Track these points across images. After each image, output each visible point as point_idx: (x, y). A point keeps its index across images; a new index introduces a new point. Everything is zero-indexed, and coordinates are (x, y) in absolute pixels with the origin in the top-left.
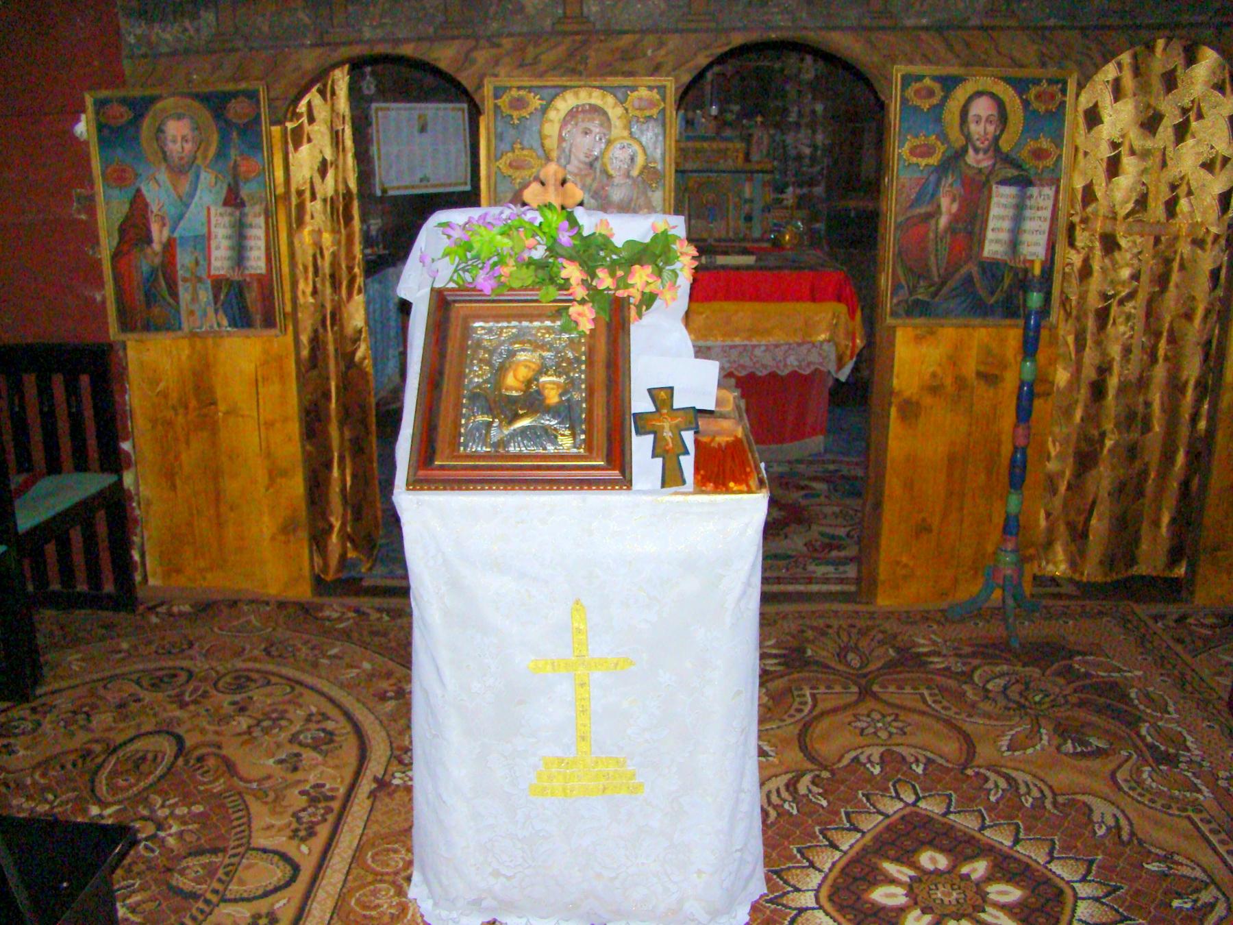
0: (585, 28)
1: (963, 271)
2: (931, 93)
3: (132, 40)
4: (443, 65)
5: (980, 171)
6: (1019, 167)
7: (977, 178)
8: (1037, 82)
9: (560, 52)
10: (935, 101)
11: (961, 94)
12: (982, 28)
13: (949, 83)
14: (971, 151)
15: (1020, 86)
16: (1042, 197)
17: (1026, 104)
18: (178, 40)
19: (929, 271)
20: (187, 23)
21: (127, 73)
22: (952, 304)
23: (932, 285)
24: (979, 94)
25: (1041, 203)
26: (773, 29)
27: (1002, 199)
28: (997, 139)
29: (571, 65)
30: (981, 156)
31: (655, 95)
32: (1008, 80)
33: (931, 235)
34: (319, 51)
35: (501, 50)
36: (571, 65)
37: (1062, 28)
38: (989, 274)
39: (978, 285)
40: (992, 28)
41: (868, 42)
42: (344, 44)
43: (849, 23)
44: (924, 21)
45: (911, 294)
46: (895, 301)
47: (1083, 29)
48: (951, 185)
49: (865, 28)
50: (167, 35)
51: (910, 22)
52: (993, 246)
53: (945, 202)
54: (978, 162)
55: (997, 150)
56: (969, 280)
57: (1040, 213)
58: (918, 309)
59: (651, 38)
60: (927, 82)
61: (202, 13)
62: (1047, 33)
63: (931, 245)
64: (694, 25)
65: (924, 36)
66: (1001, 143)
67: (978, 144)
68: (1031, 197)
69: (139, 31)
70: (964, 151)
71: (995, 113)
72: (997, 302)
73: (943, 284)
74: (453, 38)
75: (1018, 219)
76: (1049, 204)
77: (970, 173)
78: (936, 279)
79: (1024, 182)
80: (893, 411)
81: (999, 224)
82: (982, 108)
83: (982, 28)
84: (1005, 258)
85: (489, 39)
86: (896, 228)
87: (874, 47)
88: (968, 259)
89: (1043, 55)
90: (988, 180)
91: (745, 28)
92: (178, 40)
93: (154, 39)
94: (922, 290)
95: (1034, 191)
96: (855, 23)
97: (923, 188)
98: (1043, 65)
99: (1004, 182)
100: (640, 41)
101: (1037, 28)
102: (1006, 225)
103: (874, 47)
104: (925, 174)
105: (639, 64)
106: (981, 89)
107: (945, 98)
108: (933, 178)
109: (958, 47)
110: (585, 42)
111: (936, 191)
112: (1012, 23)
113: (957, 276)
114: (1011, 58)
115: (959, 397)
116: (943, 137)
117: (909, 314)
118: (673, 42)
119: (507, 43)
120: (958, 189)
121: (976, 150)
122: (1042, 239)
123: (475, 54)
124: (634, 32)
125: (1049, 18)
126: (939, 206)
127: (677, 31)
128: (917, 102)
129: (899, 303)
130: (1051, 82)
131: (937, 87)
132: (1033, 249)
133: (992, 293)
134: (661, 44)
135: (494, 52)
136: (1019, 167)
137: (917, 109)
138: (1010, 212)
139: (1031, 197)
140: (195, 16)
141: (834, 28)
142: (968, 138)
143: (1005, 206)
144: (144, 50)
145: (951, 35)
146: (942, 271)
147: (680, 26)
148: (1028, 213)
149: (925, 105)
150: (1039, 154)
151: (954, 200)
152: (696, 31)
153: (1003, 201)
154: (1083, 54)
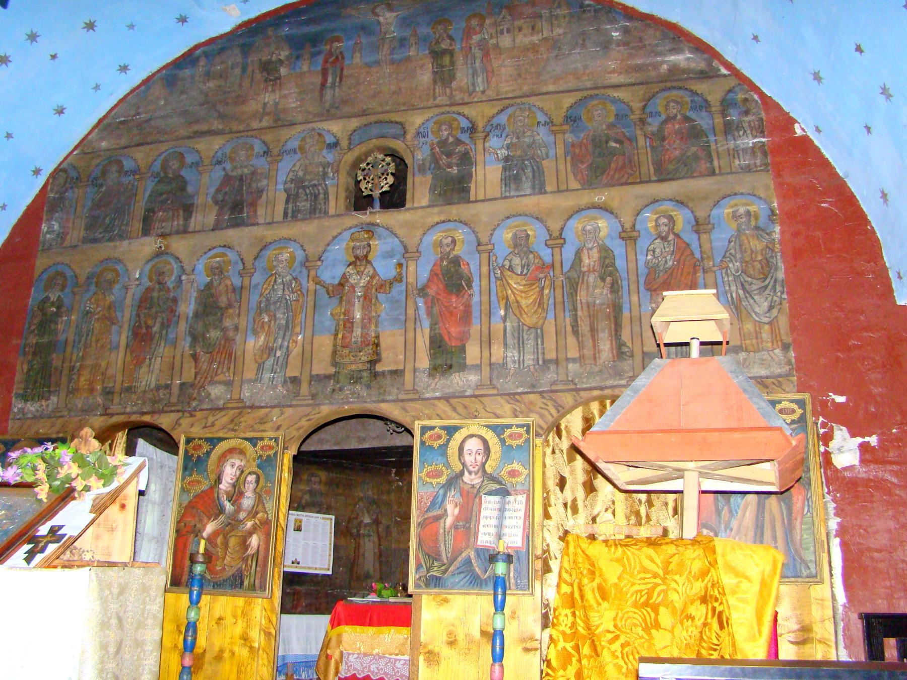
0: (240, 405)
1: (464, 555)
2: (439, 437)
3: (16, 410)
4: (164, 427)
5: (473, 486)
6: (500, 483)
7: (471, 490)
8: (509, 426)
9: (226, 419)
10: (441, 442)
11: (458, 437)
12: (476, 396)
13: (451, 430)
14: (466, 473)
15: (498, 430)
16: (517, 503)
17: (503, 441)
18: (38, 411)
19: (440, 555)
20: (43, 402)
21: (9, 428)
22: (457, 579)
23: (443, 565)
24: (471, 436)
25: (516, 506)
26: (348, 403)
27: (490, 503)
28: (483, 464)
29: (231, 426)
30: (473, 476)
31: (273, 443)
32: (488, 426)
33: (441, 531)
34: (102, 418)
35: (196, 418)
36: (231, 426)
37: (527, 393)
38: (482, 557)
39: (475, 565)
40: (482, 396)
41: (404, 409)
42: (117, 414)
43: (391, 398)
44: (437, 394)
45: (428, 571)
46: (417, 577)
47: (541, 393)
48: (453, 496)
49: (403, 401)
50: (32, 407)
51: (428, 395)
52: (485, 537)
53: (450, 507)
54: (472, 480)
55: (484, 471)
56: (468, 562)
57: (515, 514)
58: (432, 582)
59: (276, 411)
60: (437, 430)
61: (52, 397)
62: (517, 397)
63: (441, 538)
64: (300, 403)
65: (436, 402)
66: (486, 466)
67: (471, 468)
68: (509, 502)
69: (20, 406)
70: (462, 473)
71: (482, 447)
72: (489, 577)
73: (450, 565)
74: (172, 411)
75: (501, 518)
76: (522, 507)
77: (465, 487)
78: (445, 561)
79: (504, 492)
80: (421, 658)
81: (488, 522)
82: (473, 445)
83: (476, 396)
84: (493, 545)
85: (189, 412)
86: (419, 524)
87: (407, 411)
88: (468, 546)
89: (515, 410)
90: (478, 491)
91: (331, 404)
92: (38, 411)
93: (26, 410)
94: (435, 569)
95: (510, 498)
96: (395, 398)
97: (436, 498)
98: (516, 416)
99: (490, 493)
100: (270, 412)
101: (509, 394)
102: (494, 522)
103: (407, 411)
104: (437, 490)
105: (269, 425)
106: (470, 433)
107: (448, 441)
108: (441, 492)
109: (460, 409)
110: (240, 414)
111: (443, 501)
112: (494, 392)
113: (460, 559)
114: (494, 414)
115: (469, 650)
116: (448, 465)
117: (427, 585)
118: (289, 411)
119: (199, 414)
120: (458, 498)
121: (470, 473)
122: (519, 532)
123: (181, 421)
124: (267, 407)
125: (517, 388)
126: (446, 511)
127: (291, 406)
128: (431, 443)
129: (420, 578)
130: (518, 426)
131: (443, 433)
132: (513, 539)
133: (486, 572)
134: (282, 414)
135: (191, 419)
136: (500, 483)
137: (431, 447)
138: (495, 513)
139: (509, 502)
140: (48, 399)
141: (383, 401)
142: (464, 464)
143: (491, 509)
144: (21, 415)
145: (453, 401)
146: (449, 555)
147: (294, 403)
148: (507, 514)
149: (436, 444)
150: (513, 474)
151: (456, 506)
152: (302, 405)
153: (490, 506)
154: (542, 408)
